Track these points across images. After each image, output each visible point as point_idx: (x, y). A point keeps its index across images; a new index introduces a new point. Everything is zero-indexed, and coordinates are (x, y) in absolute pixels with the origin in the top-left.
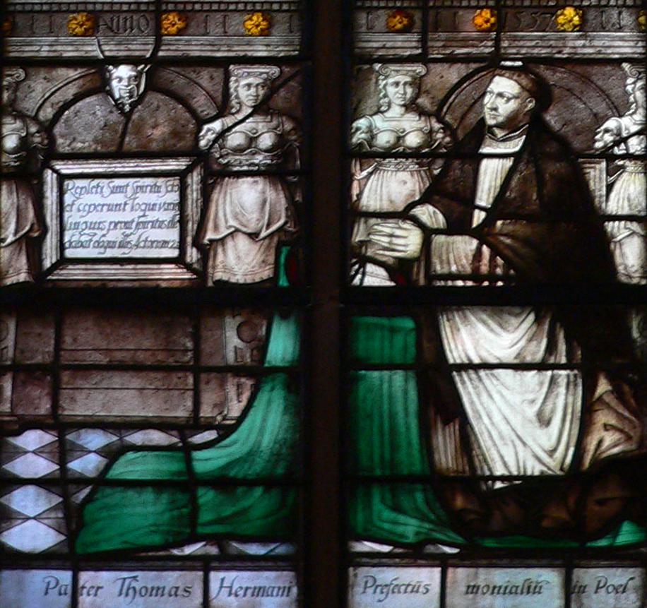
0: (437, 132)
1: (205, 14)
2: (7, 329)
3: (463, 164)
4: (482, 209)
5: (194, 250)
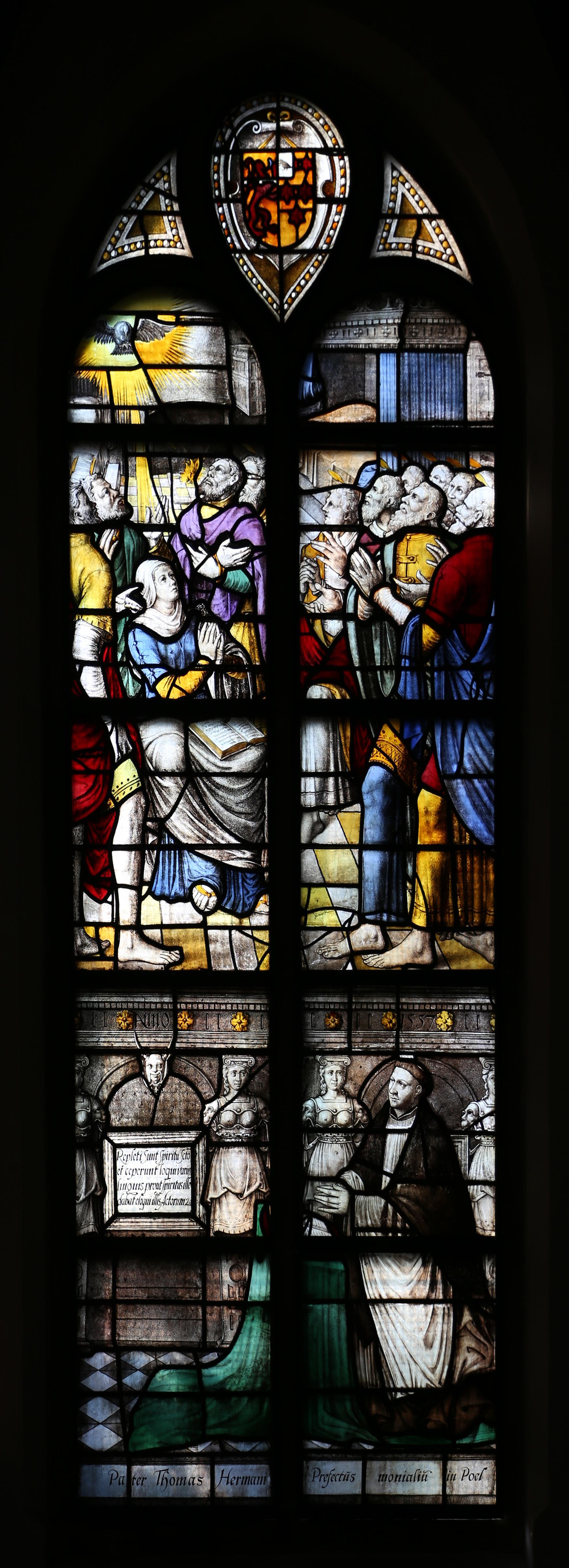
1: (205, 1013)
3: (375, 1138)
4: (387, 1174)
5: (201, 1207)
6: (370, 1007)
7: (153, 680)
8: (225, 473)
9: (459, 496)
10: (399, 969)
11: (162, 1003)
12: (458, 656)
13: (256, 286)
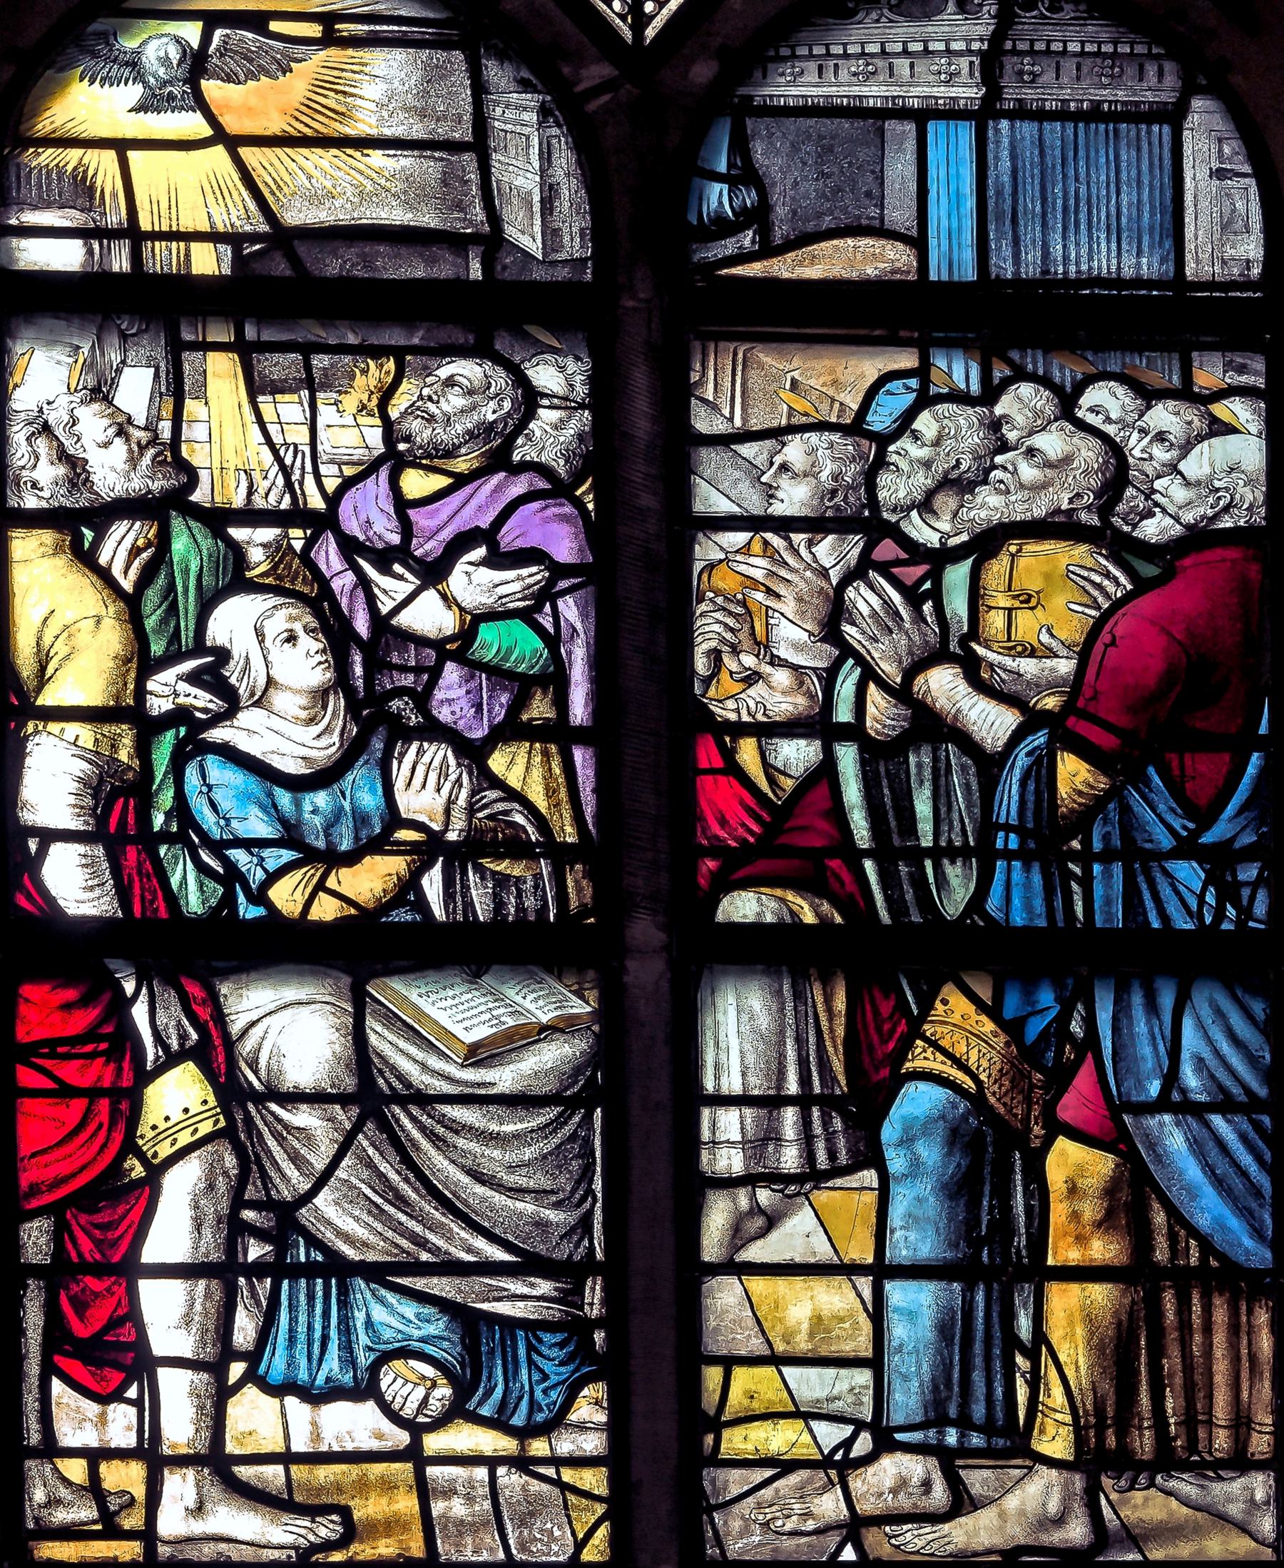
7: (260, 875)
8: (470, 392)
9: (1161, 454)
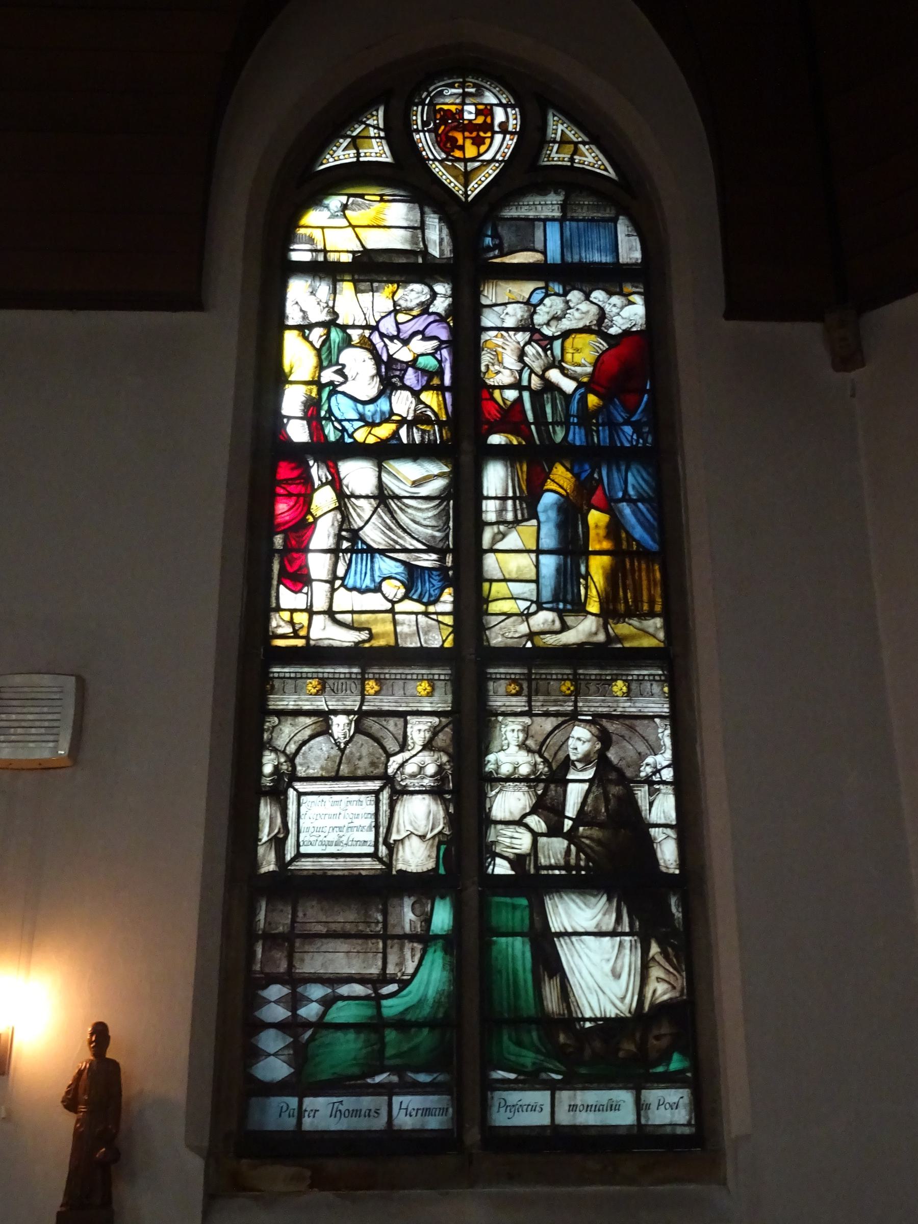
0: (539, 764)
2: (261, 907)
3: (556, 787)
5: (384, 847)
6: (549, 677)
8: (418, 293)
9: (615, 310)
10: (575, 646)
11: (351, 673)
12: (619, 415)
13: (446, 180)
